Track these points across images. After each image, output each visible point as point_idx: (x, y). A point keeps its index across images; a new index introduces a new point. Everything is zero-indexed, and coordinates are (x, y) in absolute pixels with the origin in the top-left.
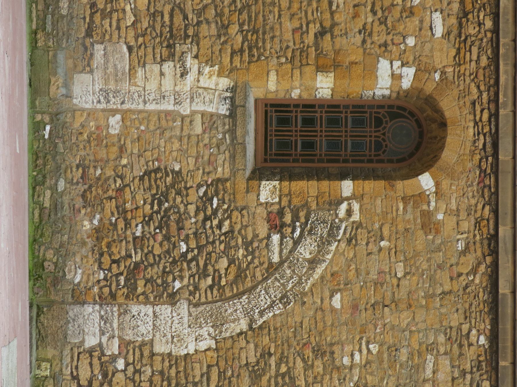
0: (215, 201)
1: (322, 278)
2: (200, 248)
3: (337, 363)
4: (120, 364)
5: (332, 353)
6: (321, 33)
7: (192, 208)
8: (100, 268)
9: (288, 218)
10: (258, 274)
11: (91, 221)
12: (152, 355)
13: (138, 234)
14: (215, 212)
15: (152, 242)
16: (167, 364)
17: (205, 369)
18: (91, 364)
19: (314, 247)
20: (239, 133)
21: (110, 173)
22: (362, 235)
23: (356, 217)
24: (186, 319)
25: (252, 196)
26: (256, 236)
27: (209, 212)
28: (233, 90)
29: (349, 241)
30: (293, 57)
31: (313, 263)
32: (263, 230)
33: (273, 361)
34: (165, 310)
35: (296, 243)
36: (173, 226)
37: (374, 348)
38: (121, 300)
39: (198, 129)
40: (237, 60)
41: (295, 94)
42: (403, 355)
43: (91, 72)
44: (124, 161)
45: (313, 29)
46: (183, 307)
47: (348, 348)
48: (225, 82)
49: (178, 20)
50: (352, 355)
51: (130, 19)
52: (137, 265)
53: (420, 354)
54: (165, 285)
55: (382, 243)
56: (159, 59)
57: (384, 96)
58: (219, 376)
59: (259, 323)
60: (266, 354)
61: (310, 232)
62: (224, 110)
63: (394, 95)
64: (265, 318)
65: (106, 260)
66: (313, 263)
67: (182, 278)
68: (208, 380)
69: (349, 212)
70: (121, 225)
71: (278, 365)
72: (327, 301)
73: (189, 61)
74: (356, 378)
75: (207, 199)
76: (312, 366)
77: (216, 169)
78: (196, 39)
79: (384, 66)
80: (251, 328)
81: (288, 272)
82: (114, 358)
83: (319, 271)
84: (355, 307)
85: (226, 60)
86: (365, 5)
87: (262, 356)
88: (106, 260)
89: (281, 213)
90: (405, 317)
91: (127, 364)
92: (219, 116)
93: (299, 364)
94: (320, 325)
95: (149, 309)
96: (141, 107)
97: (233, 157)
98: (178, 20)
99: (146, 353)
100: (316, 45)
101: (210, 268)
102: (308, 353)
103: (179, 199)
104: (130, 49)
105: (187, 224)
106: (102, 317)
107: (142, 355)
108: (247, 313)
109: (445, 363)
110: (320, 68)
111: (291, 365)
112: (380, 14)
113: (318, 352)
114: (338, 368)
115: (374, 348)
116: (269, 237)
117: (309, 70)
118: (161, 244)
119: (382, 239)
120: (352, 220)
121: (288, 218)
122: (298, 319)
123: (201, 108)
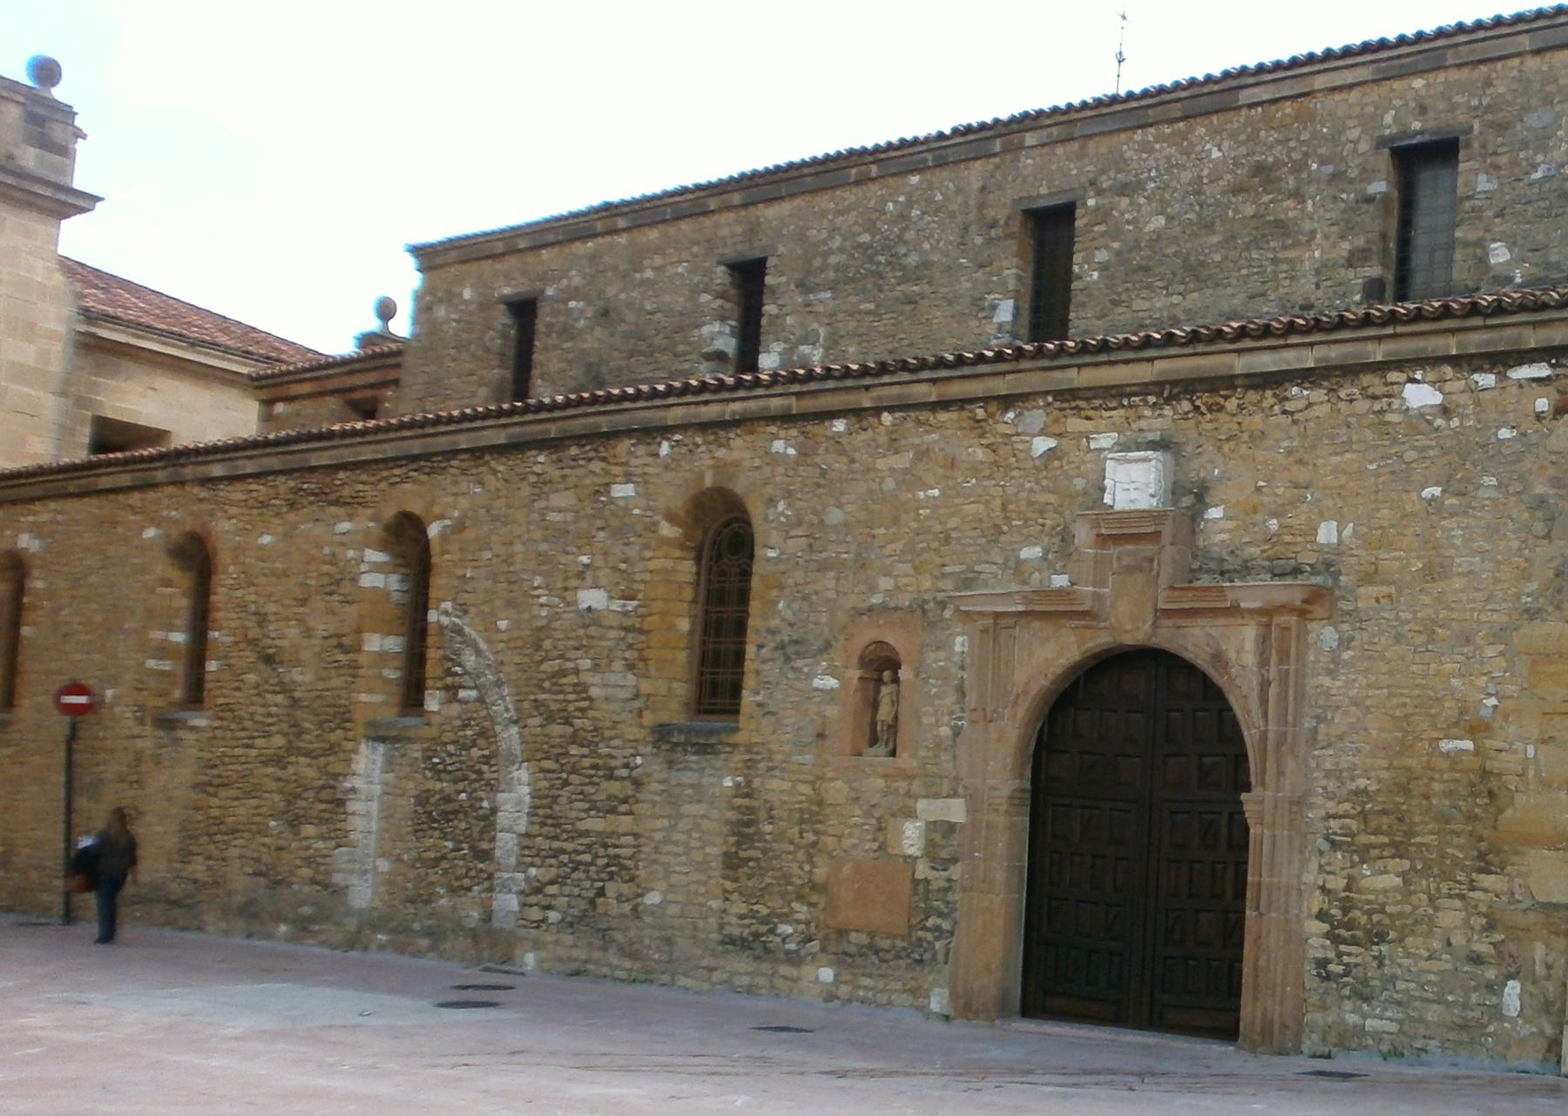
0: (436, 760)
1: (488, 641)
2: (465, 779)
3: (544, 623)
4: (533, 871)
5: (540, 629)
6: (340, 646)
7: (438, 786)
8: (469, 889)
9: (449, 680)
10: (483, 713)
11: (442, 897)
12: (527, 835)
13: (450, 845)
14: (443, 762)
15: (458, 832)
16: (535, 819)
17: (541, 775)
18: (531, 906)
19: (468, 651)
20: (393, 733)
21: (412, 874)
22: (464, 597)
23: (447, 605)
24: (505, 795)
25: (436, 720)
26: (459, 717)
27: (441, 767)
28: (369, 738)
29: (465, 612)
30: (350, 675)
31: (479, 653)
32: (455, 709)
33: (542, 697)
34: (502, 819)
35: (466, 673)
36: (450, 807)
37: (538, 581)
38: (492, 868)
39: (390, 776)
40: (350, 734)
41: (392, 674)
42: (544, 547)
43: (347, 887)
44: (406, 857)
45: (341, 657)
46: (501, 797)
47: (535, 611)
48: (364, 748)
49: (324, 795)
50: (542, 605)
51: (321, 844)
52: (472, 848)
53: (547, 529)
54: (485, 818)
55: (468, 575)
56: (343, 817)
57: (402, 581)
58: (548, 758)
59: (512, 713)
60: (538, 704)
61: (459, 655)
62: (381, 748)
63: (403, 570)
64: (510, 706)
65: (466, 882)
66: (479, 653)
67: (481, 800)
68: (549, 771)
69: (446, 613)
70: (445, 864)
71: (544, 691)
72: (503, 636)
73: (348, 785)
74: (557, 600)
75: (433, 768)
76: (546, 651)
77: (416, 759)
78: (336, 776)
79: (370, 580)
80: (516, 722)
81: (482, 679)
82: (527, 879)
83: (483, 646)
84: (511, 604)
85: (349, 745)
86: (327, 601)
87: (537, 708)
88: (466, 882)
89: (447, 688)
90: (518, 547)
91: (533, 865)
92: (384, 755)
93: (545, 667)
94: (519, 643)
95: (499, 835)
96: (373, 836)
97: (410, 740)
98: (324, 795)
99: (526, 842)
100: (347, 652)
101: (477, 768)
102: (538, 656)
103: (432, 800)
104: (339, 846)
105: (447, 791)
106: (501, 891)
107: (528, 847)
108: (506, 727)
109: (558, 500)
110: (359, 650)
111: (543, 676)
112: (333, 587)
113: (538, 647)
114: (550, 622)
115: (538, 581)
116: (461, 701)
117: (362, 659)
118: (460, 821)
119: (464, 576)
120: (450, 610)
121: (449, 680)
122: (514, 668)
123: (377, 772)
